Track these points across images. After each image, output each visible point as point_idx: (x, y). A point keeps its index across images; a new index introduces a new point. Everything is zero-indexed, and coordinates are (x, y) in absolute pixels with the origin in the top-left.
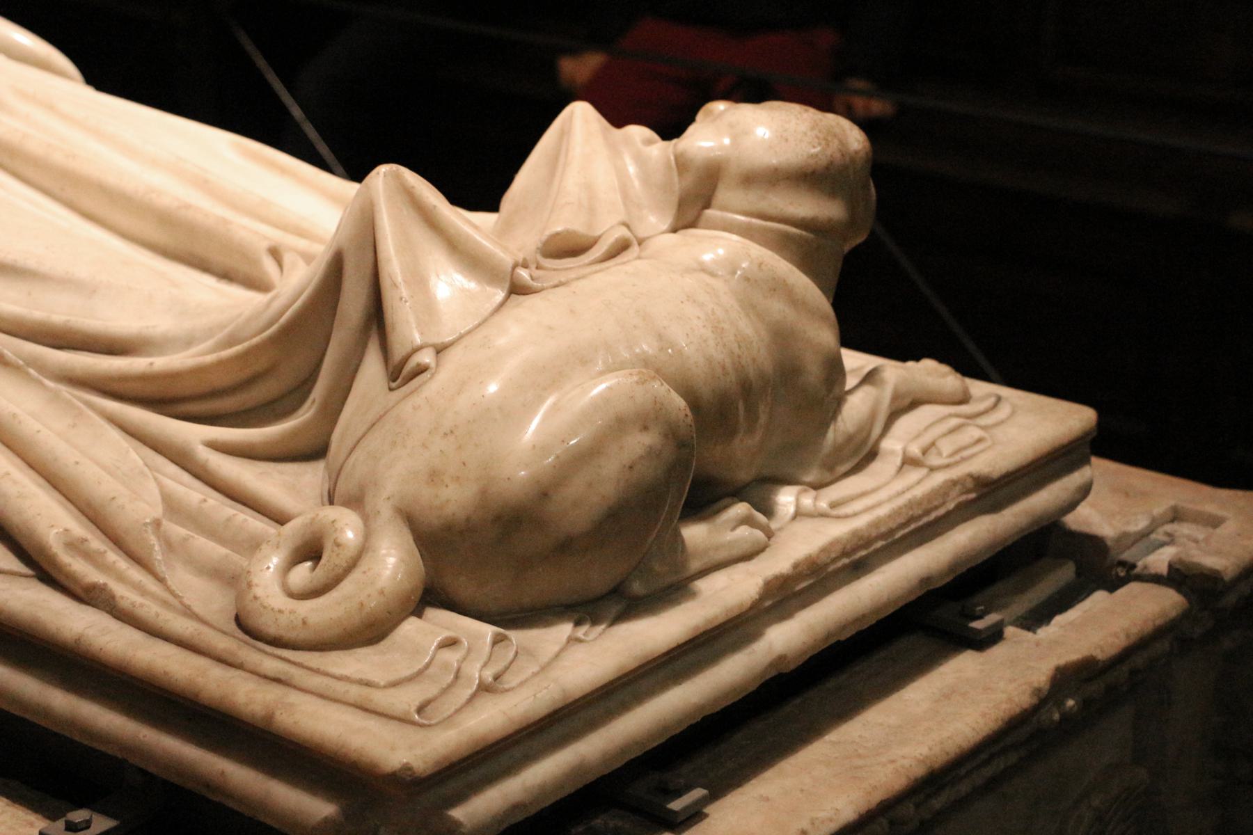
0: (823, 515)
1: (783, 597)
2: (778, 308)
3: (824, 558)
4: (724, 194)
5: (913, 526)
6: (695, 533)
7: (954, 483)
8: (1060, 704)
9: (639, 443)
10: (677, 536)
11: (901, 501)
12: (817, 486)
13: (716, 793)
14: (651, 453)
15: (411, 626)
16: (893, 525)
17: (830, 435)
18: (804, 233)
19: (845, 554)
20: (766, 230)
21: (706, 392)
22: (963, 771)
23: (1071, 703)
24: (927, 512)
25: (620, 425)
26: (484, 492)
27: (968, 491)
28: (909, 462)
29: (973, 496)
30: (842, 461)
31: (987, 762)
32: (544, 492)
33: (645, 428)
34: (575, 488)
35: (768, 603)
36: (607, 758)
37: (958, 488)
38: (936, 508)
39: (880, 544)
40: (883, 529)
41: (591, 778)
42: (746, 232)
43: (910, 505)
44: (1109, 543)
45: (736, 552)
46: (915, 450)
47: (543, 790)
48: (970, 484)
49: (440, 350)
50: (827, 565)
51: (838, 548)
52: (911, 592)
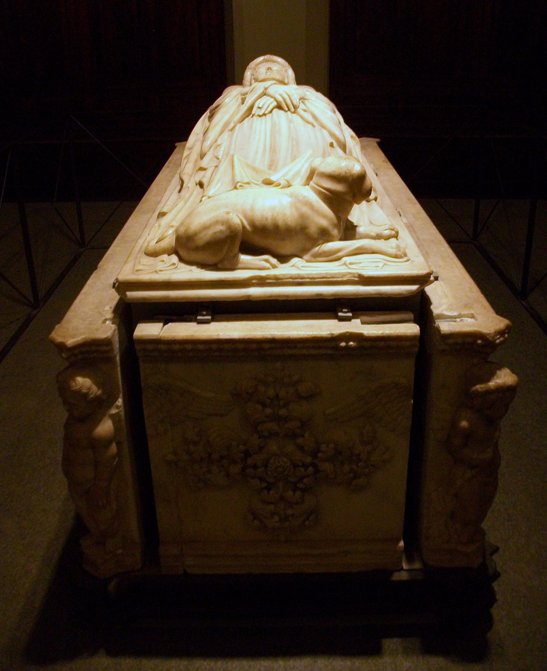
0: (299, 268)
1: (262, 282)
2: (305, 210)
3: (281, 277)
4: (315, 178)
5: (324, 280)
6: (244, 258)
7: (350, 273)
8: (347, 342)
9: (220, 228)
10: (236, 257)
11: (325, 272)
12: (307, 261)
13: (213, 320)
14: (221, 231)
15: (165, 257)
16: (315, 276)
17: (317, 249)
18: (326, 192)
19: (291, 278)
20: (316, 189)
21: (257, 223)
22: (299, 346)
23: (351, 343)
24: (334, 278)
25: (217, 222)
26: (186, 230)
27: (355, 277)
28: (345, 264)
29: (357, 279)
30: (321, 257)
31: (314, 348)
32: (196, 234)
33: (223, 225)
34: (202, 235)
35: (254, 281)
36: (177, 298)
37: (350, 275)
38: (338, 278)
39: (308, 280)
40: (310, 276)
41: (170, 301)
42: (313, 189)
43: (327, 274)
44: (434, 315)
45: (256, 267)
46: (348, 262)
47: (154, 298)
48: (357, 275)
49: (209, 197)
50: (282, 279)
51: (289, 276)
52: (312, 296)
